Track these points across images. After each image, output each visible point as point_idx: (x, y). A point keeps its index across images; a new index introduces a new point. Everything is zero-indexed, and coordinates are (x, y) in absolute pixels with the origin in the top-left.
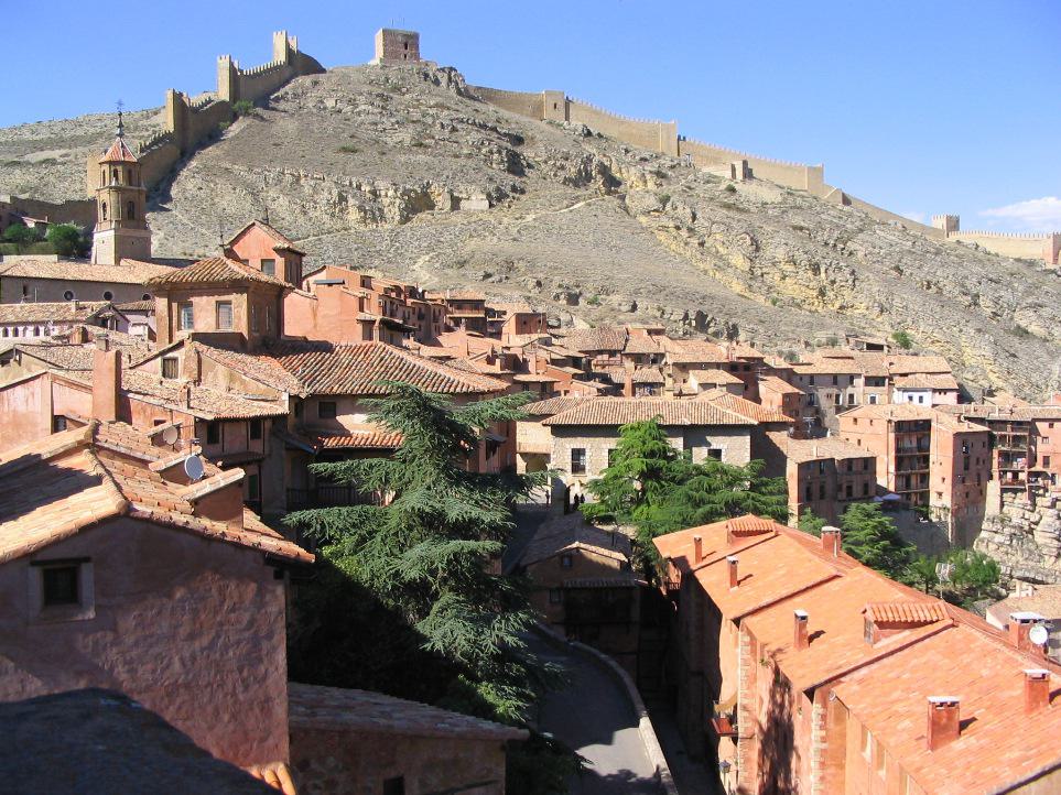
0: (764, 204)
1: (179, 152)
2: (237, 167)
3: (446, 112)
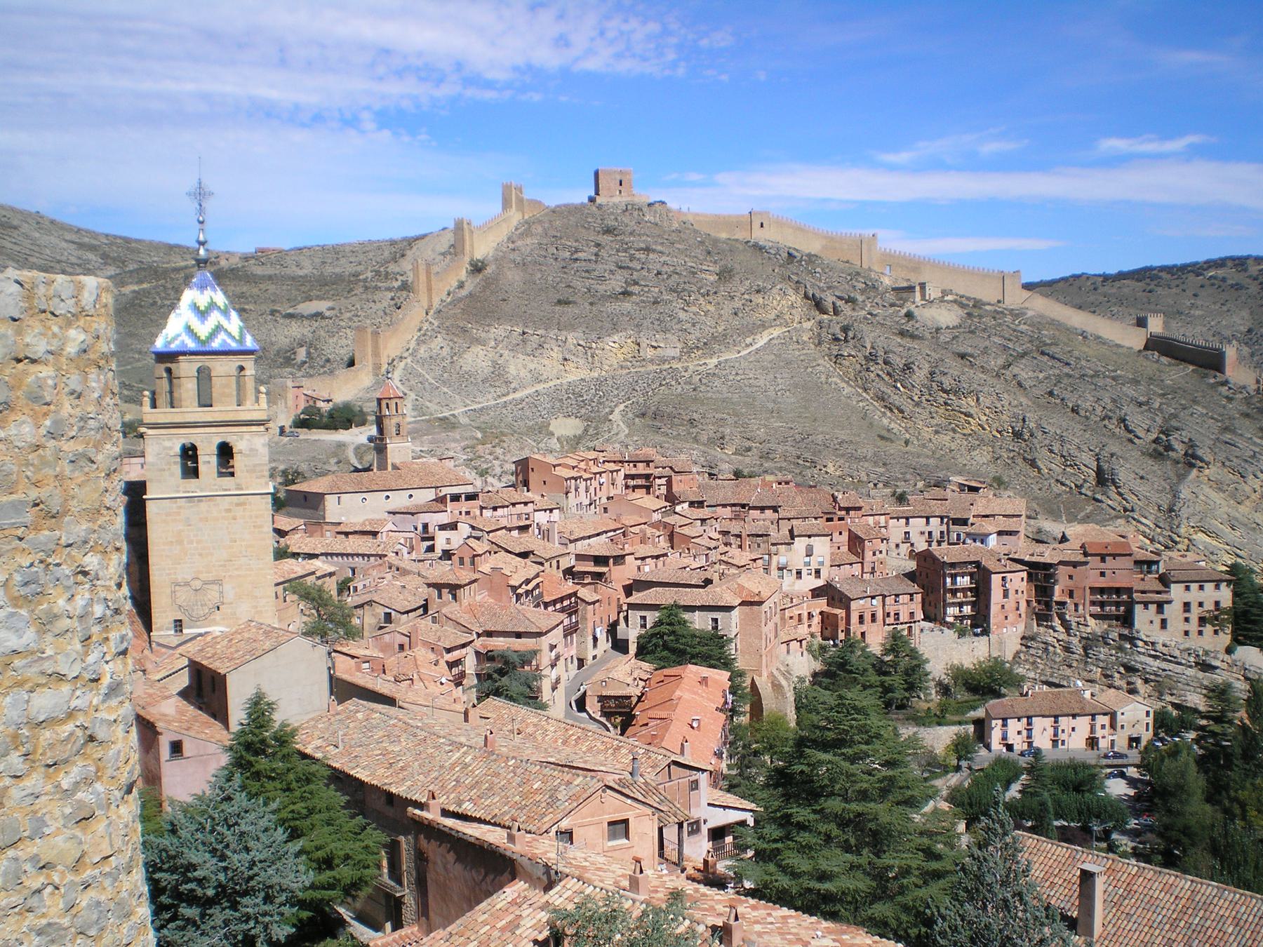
0: (938, 330)
3: (651, 256)
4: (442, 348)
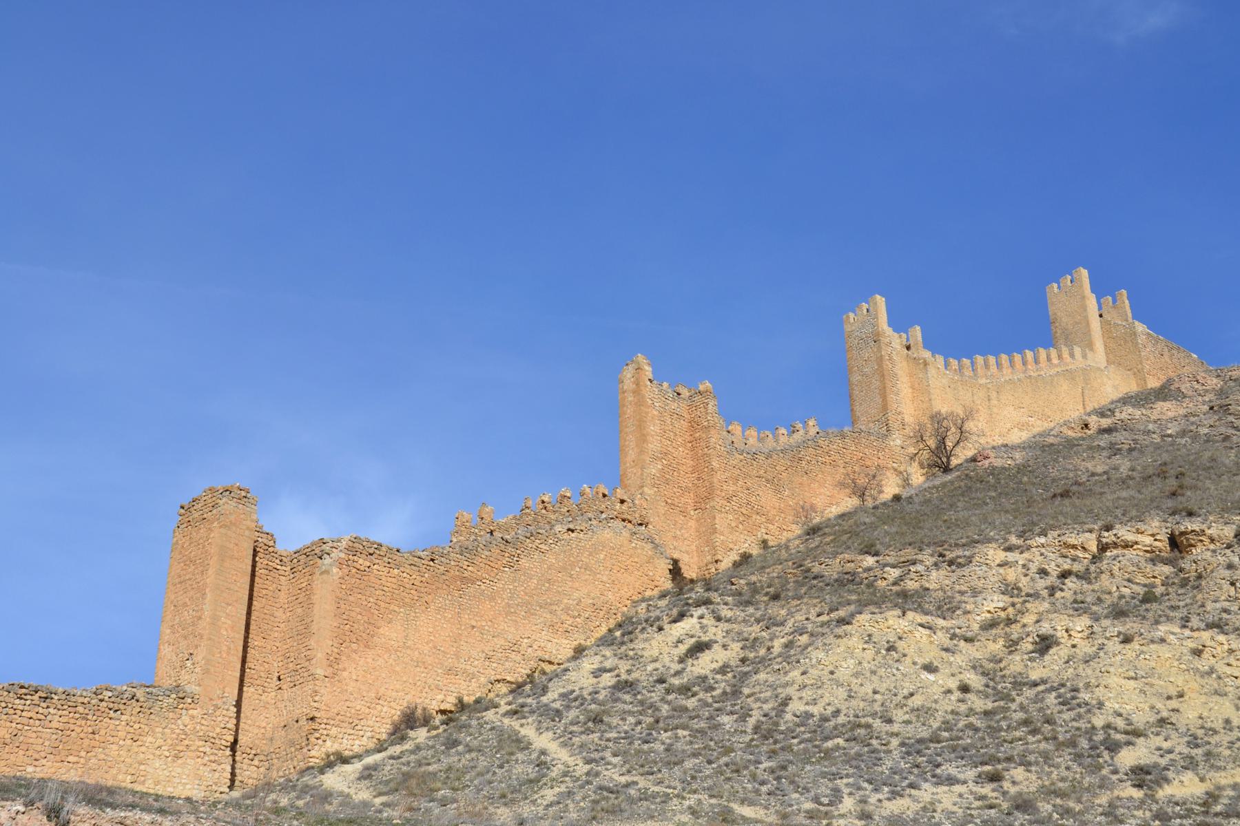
2: (870, 561)
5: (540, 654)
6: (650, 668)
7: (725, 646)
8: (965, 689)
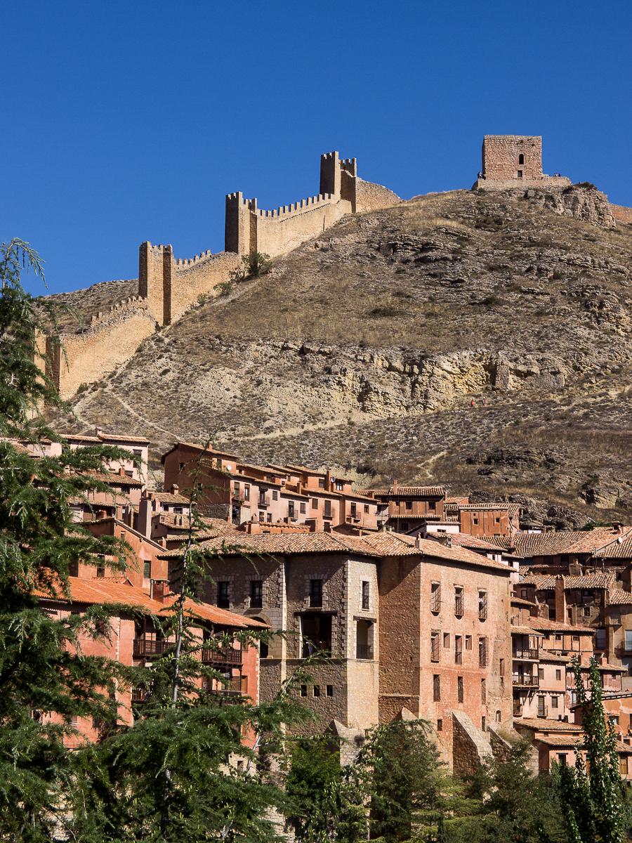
1: (154, 325)
3: (548, 252)
4: (165, 372)
5: (116, 362)
6: (152, 376)
7: (173, 372)
8: (235, 397)
